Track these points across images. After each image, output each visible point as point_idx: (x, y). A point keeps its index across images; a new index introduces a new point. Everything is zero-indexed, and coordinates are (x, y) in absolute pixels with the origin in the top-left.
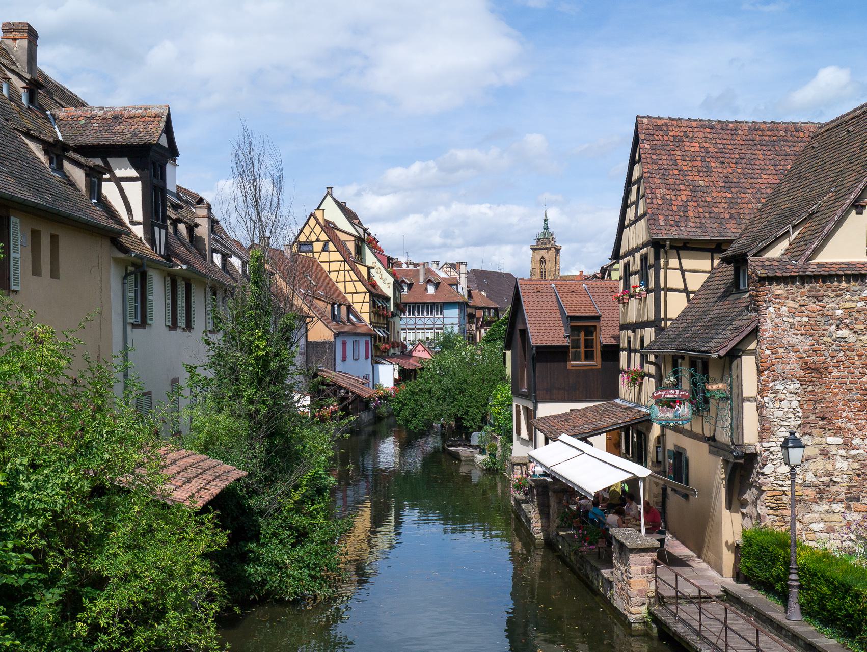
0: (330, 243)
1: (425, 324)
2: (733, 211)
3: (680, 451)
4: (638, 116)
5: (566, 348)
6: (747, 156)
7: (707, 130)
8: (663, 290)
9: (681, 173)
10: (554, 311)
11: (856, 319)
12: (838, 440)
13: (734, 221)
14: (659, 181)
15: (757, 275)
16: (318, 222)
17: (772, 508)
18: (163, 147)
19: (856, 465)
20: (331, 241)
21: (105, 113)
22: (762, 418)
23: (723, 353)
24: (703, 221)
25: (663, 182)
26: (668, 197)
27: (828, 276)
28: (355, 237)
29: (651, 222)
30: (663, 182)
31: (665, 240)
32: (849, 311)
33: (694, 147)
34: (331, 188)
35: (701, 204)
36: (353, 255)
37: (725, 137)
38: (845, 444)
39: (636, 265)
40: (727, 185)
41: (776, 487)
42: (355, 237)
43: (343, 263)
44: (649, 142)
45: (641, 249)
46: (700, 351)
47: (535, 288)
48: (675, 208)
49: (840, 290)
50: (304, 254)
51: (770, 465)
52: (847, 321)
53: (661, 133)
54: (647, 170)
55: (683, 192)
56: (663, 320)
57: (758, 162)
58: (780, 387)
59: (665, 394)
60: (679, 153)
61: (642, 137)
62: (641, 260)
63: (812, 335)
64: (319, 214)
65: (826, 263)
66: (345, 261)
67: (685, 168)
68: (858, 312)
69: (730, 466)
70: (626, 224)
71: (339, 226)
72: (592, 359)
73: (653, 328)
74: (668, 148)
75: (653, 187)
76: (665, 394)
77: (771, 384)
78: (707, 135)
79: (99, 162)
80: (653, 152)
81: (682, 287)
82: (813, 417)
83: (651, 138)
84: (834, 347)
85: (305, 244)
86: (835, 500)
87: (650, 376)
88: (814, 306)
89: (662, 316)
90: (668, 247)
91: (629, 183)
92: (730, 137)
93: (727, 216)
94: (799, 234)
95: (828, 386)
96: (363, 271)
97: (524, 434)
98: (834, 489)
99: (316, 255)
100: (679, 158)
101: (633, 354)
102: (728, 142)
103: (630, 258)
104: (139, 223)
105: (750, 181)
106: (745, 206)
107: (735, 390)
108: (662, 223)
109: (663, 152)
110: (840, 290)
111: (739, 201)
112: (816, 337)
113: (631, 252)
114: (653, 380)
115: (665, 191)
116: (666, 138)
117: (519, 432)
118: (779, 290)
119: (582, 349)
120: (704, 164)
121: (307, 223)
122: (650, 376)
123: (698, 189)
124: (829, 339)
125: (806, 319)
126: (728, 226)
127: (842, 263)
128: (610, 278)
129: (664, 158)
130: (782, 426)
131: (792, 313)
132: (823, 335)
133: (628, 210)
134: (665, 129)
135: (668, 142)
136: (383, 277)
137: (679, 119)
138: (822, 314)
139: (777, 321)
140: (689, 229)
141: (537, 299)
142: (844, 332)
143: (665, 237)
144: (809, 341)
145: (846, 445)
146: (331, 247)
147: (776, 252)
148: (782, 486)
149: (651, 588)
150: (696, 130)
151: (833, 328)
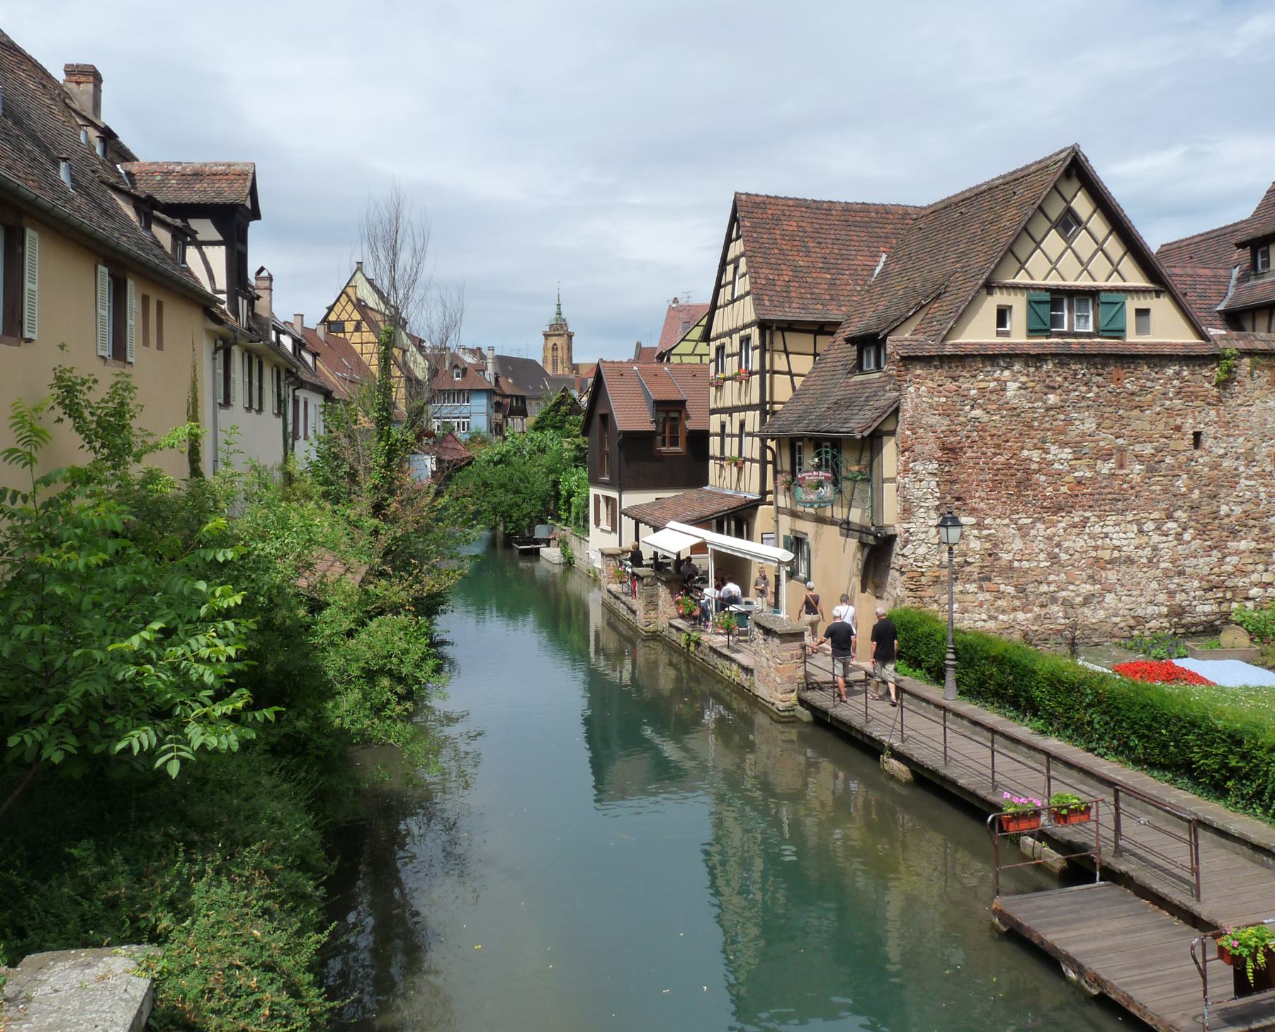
2: (833, 292)
3: (799, 535)
4: (736, 193)
6: (843, 237)
7: (803, 209)
8: (768, 372)
11: (989, 399)
12: (972, 520)
13: (834, 303)
14: (761, 260)
15: (898, 354)
17: (911, 590)
19: (988, 545)
22: (905, 500)
23: (866, 434)
25: (765, 261)
26: (771, 277)
29: (757, 302)
30: (765, 261)
33: (792, 226)
37: (820, 216)
39: (733, 345)
40: (826, 266)
41: (915, 568)
48: (778, 289)
51: (909, 546)
53: (760, 211)
55: (784, 272)
56: (768, 403)
57: (853, 243)
60: (778, 232)
62: (741, 342)
67: (785, 247)
72: (677, 445)
74: (768, 227)
77: (911, 465)
78: (804, 214)
83: (750, 215)
84: (969, 427)
86: (968, 581)
87: (752, 460)
88: (951, 386)
89: (768, 399)
90: (774, 328)
92: (825, 217)
93: (828, 297)
95: (963, 466)
97: (604, 524)
98: (968, 569)
100: (778, 237)
101: (728, 440)
102: (824, 222)
103: (726, 340)
105: (847, 262)
106: (844, 287)
108: (767, 303)
109: (764, 231)
111: (838, 282)
113: (729, 334)
115: (768, 271)
116: (764, 216)
117: (597, 523)
122: (752, 460)
124: (964, 420)
125: (944, 400)
126: (830, 307)
129: (765, 236)
130: (922, 507)
131: (931, 392)
133: (722, 290)
139: (917, 400)
142: (977, 413)
143: (772, 318)
144: (946, 422)
145: (979, 526)
150: (792, 209)
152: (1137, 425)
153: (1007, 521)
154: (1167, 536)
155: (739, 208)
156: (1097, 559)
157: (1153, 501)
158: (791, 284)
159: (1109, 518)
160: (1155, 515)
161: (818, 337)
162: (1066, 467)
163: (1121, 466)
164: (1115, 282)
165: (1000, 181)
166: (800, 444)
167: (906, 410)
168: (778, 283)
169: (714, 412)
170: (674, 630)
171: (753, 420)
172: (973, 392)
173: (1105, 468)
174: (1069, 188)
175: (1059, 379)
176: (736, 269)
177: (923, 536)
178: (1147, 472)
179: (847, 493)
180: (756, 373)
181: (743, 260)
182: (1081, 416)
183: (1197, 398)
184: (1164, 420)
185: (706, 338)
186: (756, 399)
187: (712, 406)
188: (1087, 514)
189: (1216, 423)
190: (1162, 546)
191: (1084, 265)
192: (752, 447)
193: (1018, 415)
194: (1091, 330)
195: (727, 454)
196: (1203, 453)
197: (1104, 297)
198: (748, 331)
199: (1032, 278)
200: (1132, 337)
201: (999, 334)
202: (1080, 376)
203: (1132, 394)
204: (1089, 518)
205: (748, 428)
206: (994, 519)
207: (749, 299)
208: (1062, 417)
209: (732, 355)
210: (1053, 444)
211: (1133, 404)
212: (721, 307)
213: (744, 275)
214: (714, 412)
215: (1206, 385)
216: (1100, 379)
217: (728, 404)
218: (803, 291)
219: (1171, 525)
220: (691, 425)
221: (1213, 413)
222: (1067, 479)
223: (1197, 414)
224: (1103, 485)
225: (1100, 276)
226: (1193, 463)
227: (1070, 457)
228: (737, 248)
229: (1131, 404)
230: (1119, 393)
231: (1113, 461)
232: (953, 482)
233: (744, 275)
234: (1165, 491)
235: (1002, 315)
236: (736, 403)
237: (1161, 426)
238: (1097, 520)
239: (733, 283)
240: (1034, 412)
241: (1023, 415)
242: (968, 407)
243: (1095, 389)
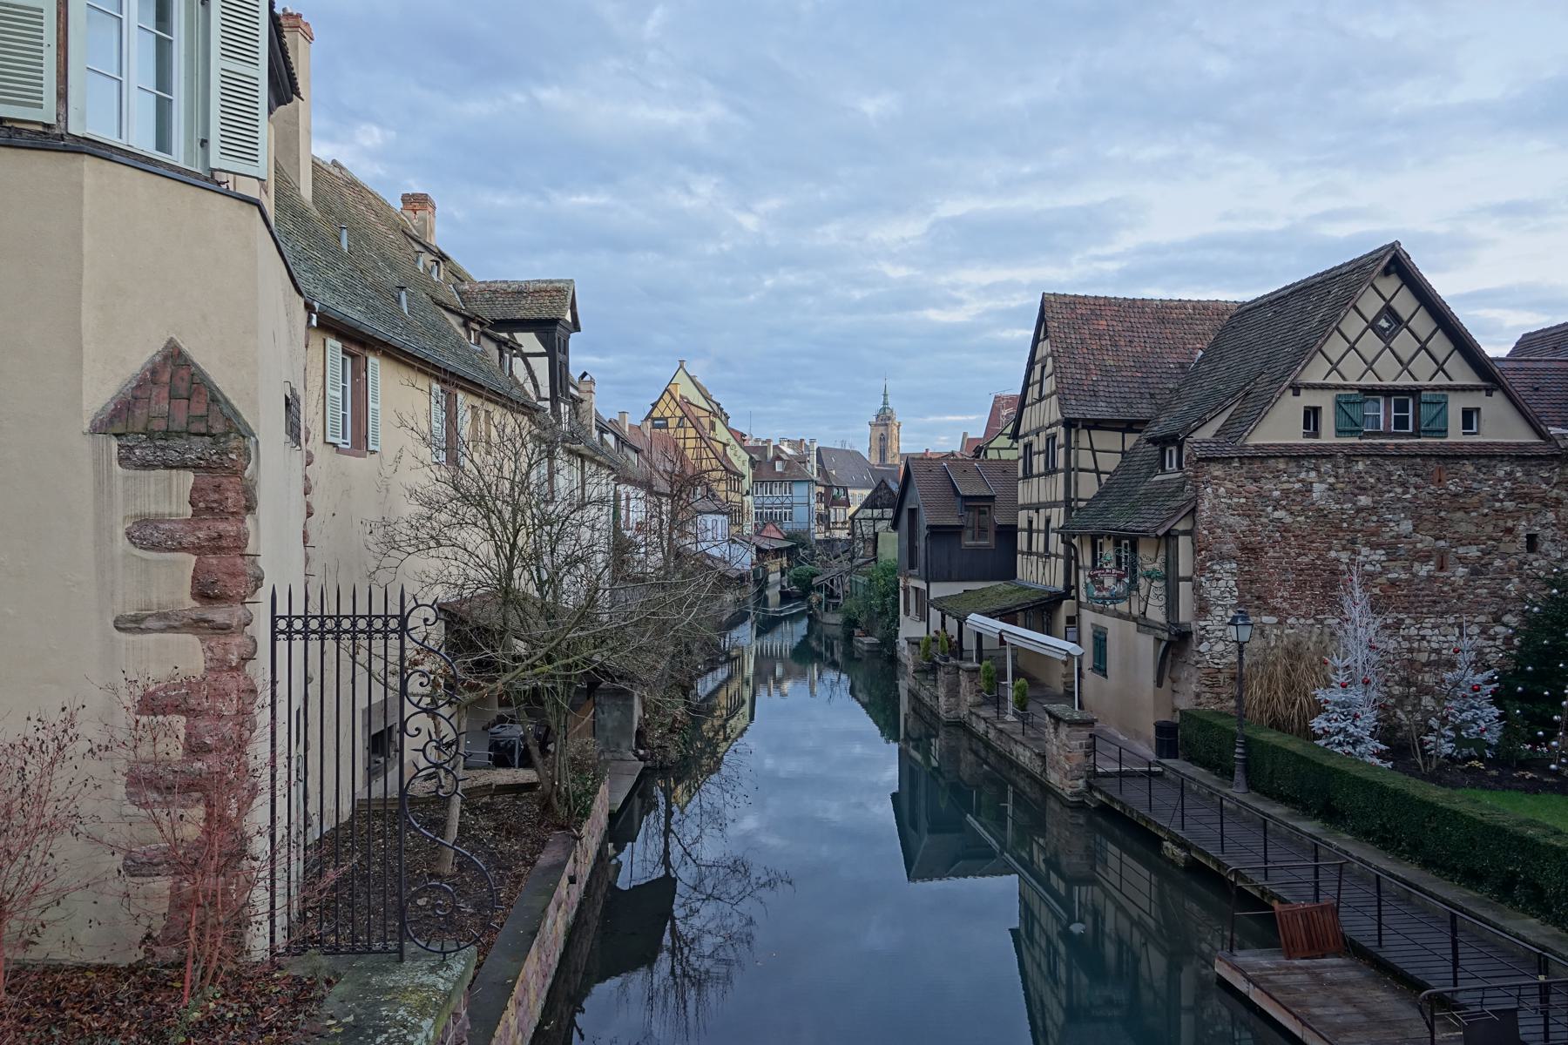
1: (773, 504)
8: (1073, 469)
11: (1293, 500)
12: (1274, 620)
13: (1144, 401)
15: (1195, 455)
16: (673, 398)
18: (566, 321)
21: (509, 287)
24: (1113, 401)
26: (1078, 376)
27: (1265, 455)
32: (1286, 493)
38: (1279, 623)
39: (1039, 444)
41: (1212, 665)
46: (1134, 531)
48: (1085, 388)
49: (1278, 471)
52: (1284, 503)
58: (1216, 567)
61: (1049, 314)
62: (1048, 440)
63: (1249, 516)
65: (1264, 445)
68: (1295, 493)
69: (1164, 644)
72: (985, 538)
77: (1208, 564)
79: (505, 335)
81: (1093, 467)
82: (1248, 597)
84: (1271, 528)
87: (1057, 556)
88: (1253, 487)
90: (1080, 426)
94: (1231, 415)
95: (1264, 566)
96: (720, 448)
101: (1035, 535)
104: (546, 399)
107: (1171, 569)
108: (1073, 402)
110: (1278, 471)
111: (1150, 380)
112: (1253, 518)
118: (1217, 470)
121: (661, 397)
122: (1057, 556)
124: (1266, 520)
125: (1243, 500)
127: (1280, 445)
131: (1230, 493)
132: (1260, 516)
133: (1030, 389)
136: (738, 454)
138: (1260, 495)
139: (1215, 501)
142: (1277, 514)
143: (1077, 416)
144: (1246, 522)
147: (1207, 433)
148: (1218, 664)
151: (1270, 509)
152: (1464, 528)
153: (1311, 621)
154: (1494, 640)
156: (1411, 662)
157: (1479, 605)
159: (1427, 620)
160: (1482, 619)
161: (1126, 435)
162: (1378, 568)
163: (1441, 568)
164: (1440, 380)
165: (1319, 279)
167: (1203, 511)
169: (1024, 507)
170: (974, 718)
171: (1058, 517)
172: (1276, 494)
173: (1423, 570)
174: (1389, 285)
175: (1372, 480)
176: (1043, 368)
177: (1220, 634)
178: (1472, 575)
179: (1143, 592)
180: (1061, 471)
182: (1396, 518)
183: (1532, 500)
184: (1494, 522)
185: (1015, 436)
186: (1061, 497)
187: (1020, 501)
188: (1400, 616)
189: (1554, 525)
190: (1488, 650)
191: (1405, 365)
192: (1057, 545)
193: (1326, 516)
194: (1410, 430)
195: (1034, 549)
196: (1538, 556)
197: (1425, 395)
198: (1054, 429)
199: (1344, 379)
200: (1456, 435)
201: (1306, 435)
202: (1395, 477)
203: (1456, 495)
204: (1403, 620)
205: (1053, 524)
206: (1298, 619)
207: (1054, 397)
208: (1375, 518)
209: (1039, 453)
210: (1364, 546)
211: (1457, 505)
214: (1024, 507)
215: (1544, 486)
216: (1419, 480)
217: (1035, 500)
218: (1111, 390)
219: (1499, 629)
220: (1000, 519)
221: (1551, 516)
222: (1379, 581)
223: (1531, 516)
224: (1420, 587)
225: (1423, 373)
226: (1526, 567)
227: (1383, 558)
228: (1044, 348)
229: (1454, 505)
230: (1441, 495)
231: (1432, 563)
232: (1251, 582)
234: (1493, 594)
235: (1312, 416)
236: (1043, 499)
237: (1489, 529)
238: (1413, 622)
240: (1343, 514)
241: (1330, 516)
242: (1271, 508)
243: (1412, 490)
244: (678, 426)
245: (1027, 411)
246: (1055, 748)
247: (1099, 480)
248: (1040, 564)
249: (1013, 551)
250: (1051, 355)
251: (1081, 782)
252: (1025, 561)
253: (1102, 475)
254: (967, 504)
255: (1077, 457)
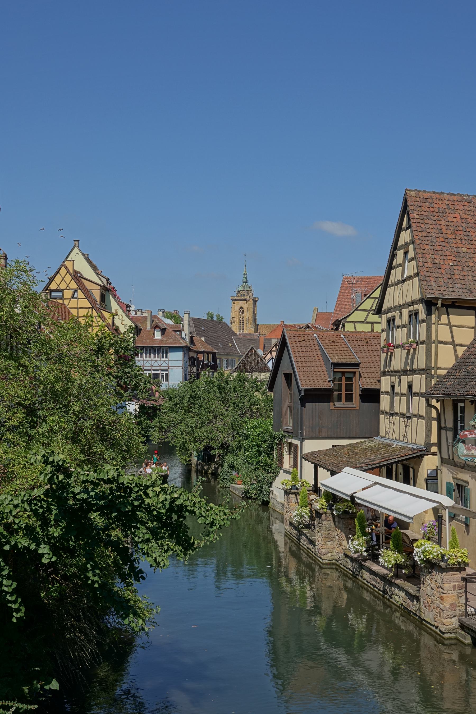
0: (79, 291)
1: (152, 366)
3: (460, 483)
5: (331, 391)
7: (466, 204)
9: (446, 240)
10: (318, 358)
16: (68, 272)
20: (80, 289)
25: (432, 248)
26: (437, 261)
28: (101, 286)
29: (424, 283)
30: (432, 248)
31: (437, 299)
34: (78, 241)
35: (466, 268)
36: (99, 302)
42: (101, 286)
43: (91, 309)
44: (417, 213)
45: (410, 306)
47: (300, 338)
50: (55, 300)
53: (427, 205)
54: (418, 237)
59: (471, 434)
60: (443, 223)
61: (410, 208)
62: (410, 316)
64: (68, 264)
66: (92, 308)
70: (390, 283)
71: (85, 276)
73: (424, 376)
75: (424, 252)
76: (471, 434)
78: (466, 208)
80: (421, 221)
85: (56, 291)
89: (433, 365)
90: (439, 305)
91: (395, 247)
99: (66, 302)
100: (443, 227)
101: (397, 398)
103: (397, 314)
108: (433, 284)
109: (430, 222)
113: (400, 308)
114: (424, 421)
115: (433, 256)
116: (431, 209)
119: (343, 392)
120: (465, 233)
123: (461, 255)
128: (344, 330)
129: (432, 227)
134: (431, 201)
135: (434, 213)
136: (125, 323)
137: (442, 193)
140: (456, 290)
141: (303, 348)
146: (80, 294)
149: (461, 602)
150: (456, 203)
155: (409, 203)
158: (456, 268)
166: (463, 405)
168: (442, 266)
170: (348, 560)
176: (406, 253)
180: (422, 343)
181: (411, 247)
185: (379, 311)
198: (416, 307)
205: (415, 389)
212: (392, 285)
213: (412, 259)
218: (465, 274)
233: (412, 259)
239: (402, 265)
244: (73, 297)
245: (390, 290)
246: (429, 588)
247: (455, 351)
248: (403, 424)
249: (378, 412)
250: (412, 242)
251: (454, 619)
252: (387, 421)
253: (458, 348)
254: (335, 370)
255: (437, 331)
